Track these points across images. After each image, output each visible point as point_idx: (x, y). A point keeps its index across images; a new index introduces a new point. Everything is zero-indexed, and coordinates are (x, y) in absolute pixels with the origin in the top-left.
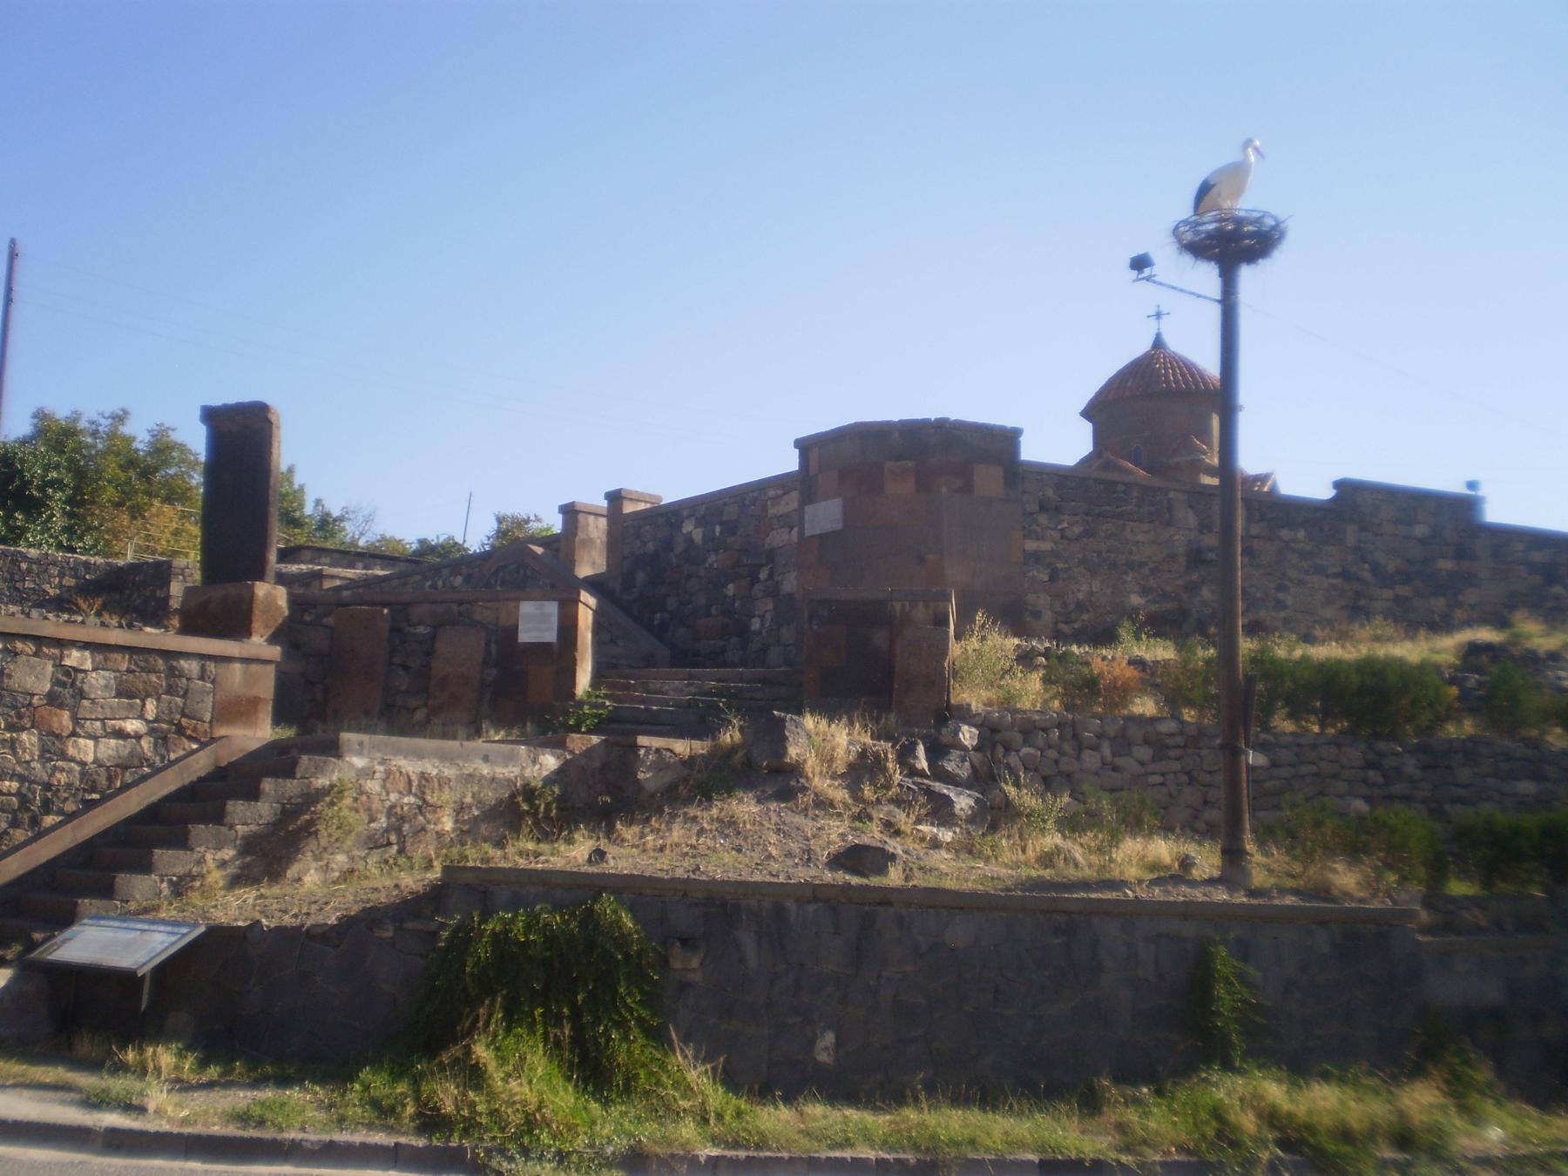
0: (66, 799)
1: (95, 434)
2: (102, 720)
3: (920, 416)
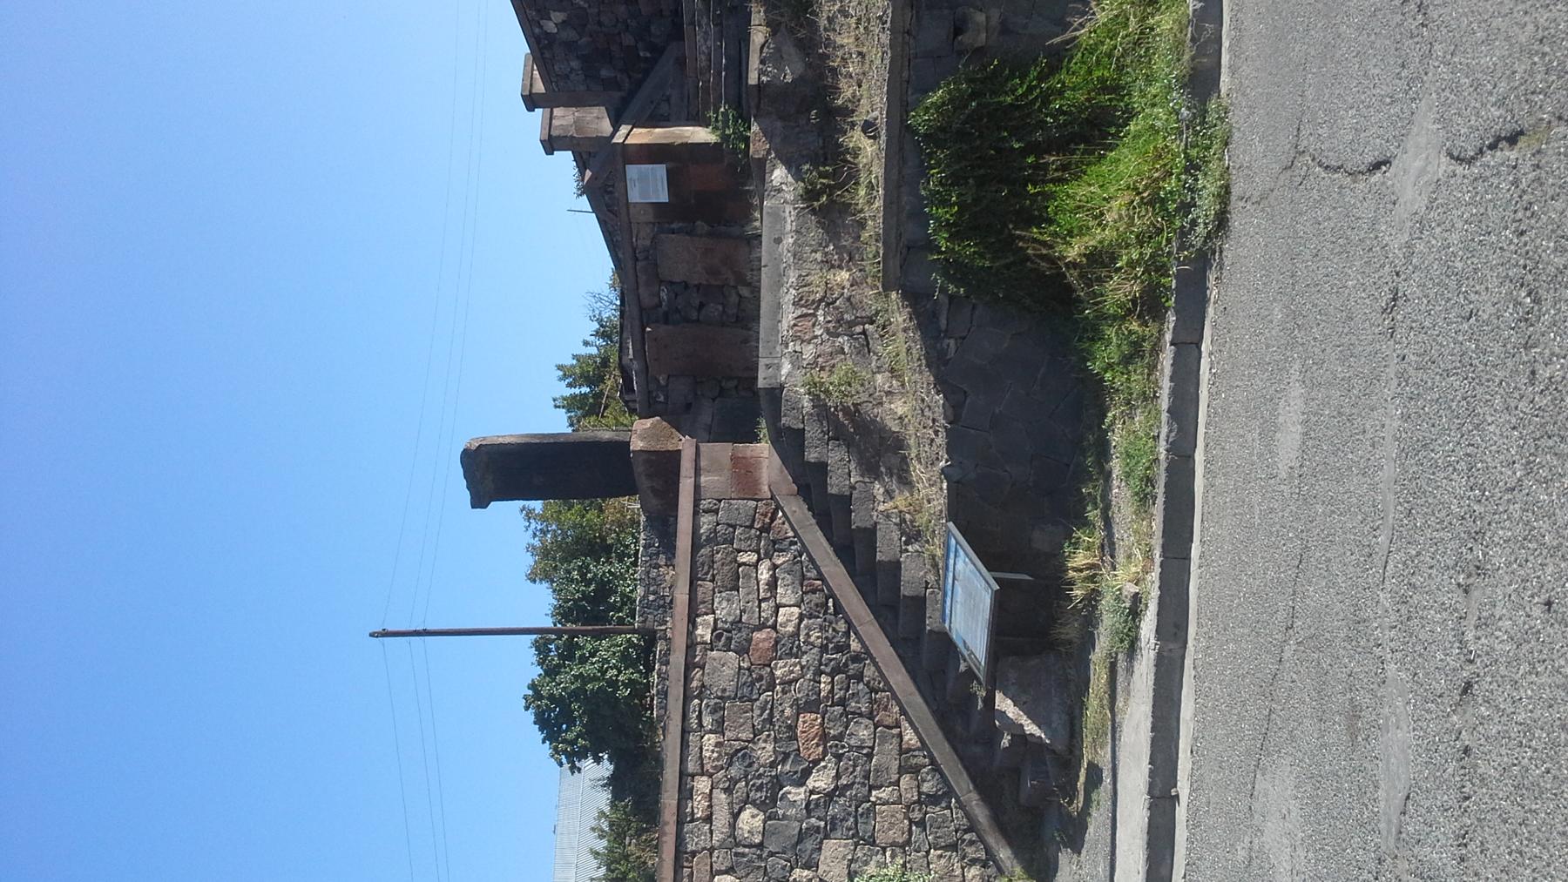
0: (834, 630)
1: (544, 532)
2: (760, 601)
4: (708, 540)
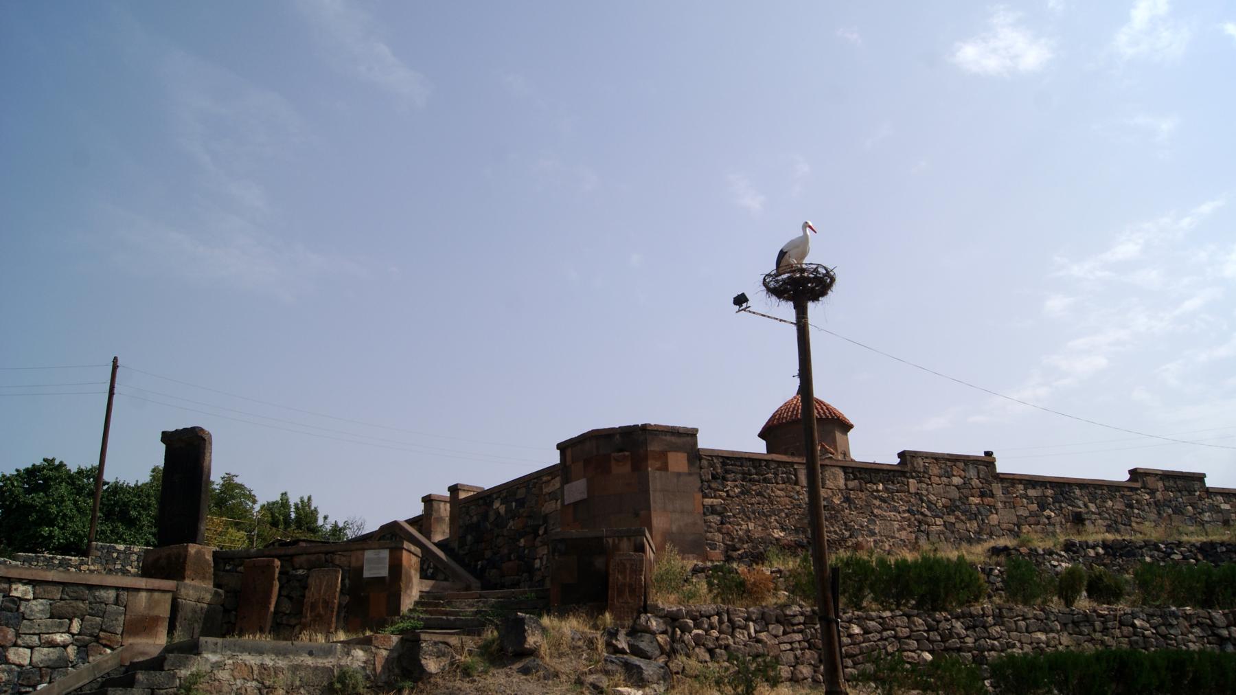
3: (632, 423)
4: (95, 597)
